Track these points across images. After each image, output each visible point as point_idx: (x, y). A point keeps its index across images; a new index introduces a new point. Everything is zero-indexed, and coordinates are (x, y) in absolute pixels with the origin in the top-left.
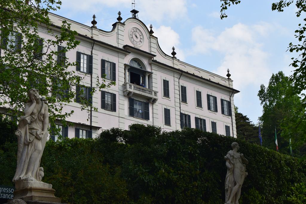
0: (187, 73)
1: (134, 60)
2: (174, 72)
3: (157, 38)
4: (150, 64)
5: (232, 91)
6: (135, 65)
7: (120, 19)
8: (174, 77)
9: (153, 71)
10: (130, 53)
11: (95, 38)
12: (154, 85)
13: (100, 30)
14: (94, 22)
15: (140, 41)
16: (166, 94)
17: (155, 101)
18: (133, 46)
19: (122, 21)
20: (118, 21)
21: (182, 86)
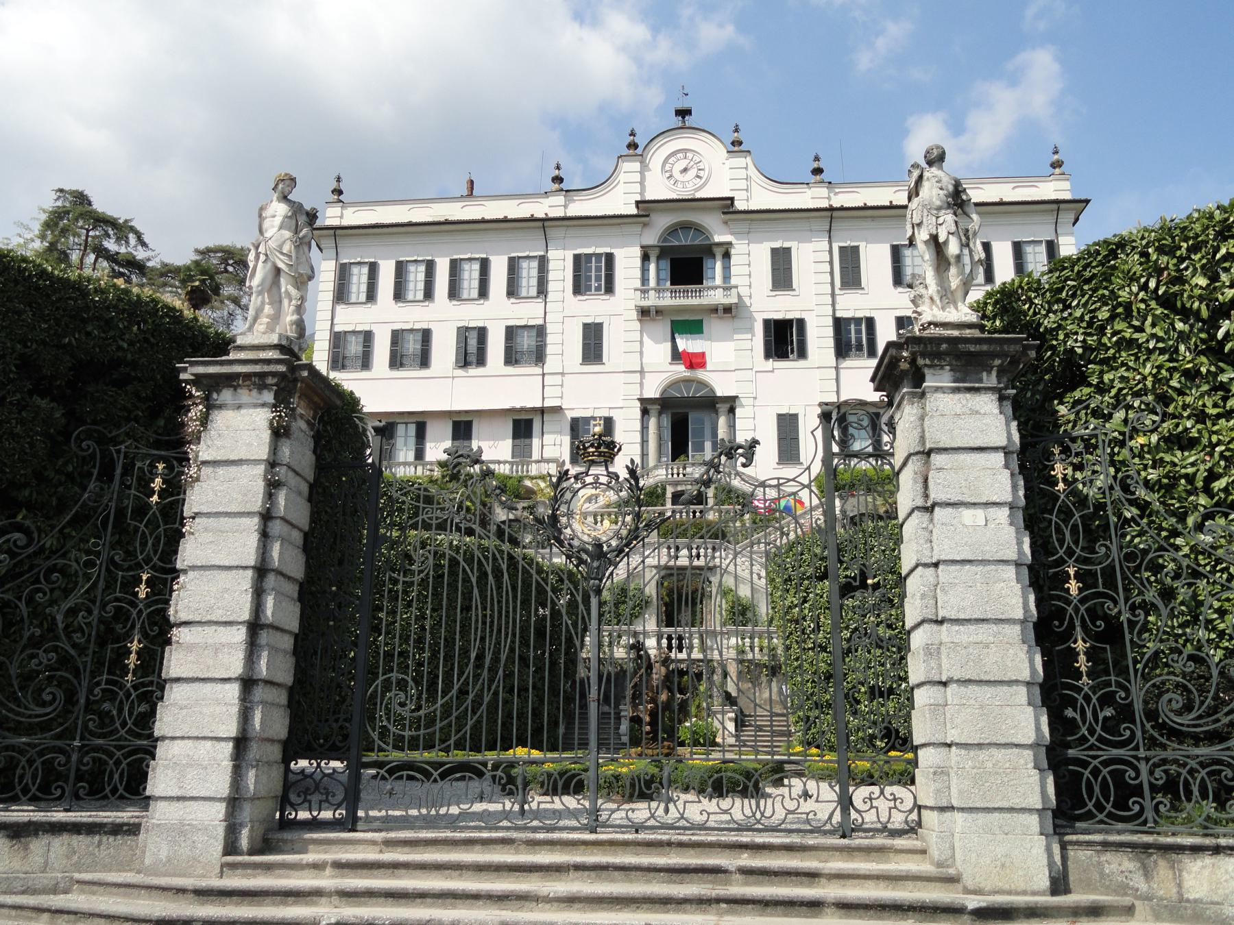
2: (808, 218)
3: (749, 152)
4: (726, 223)
5: (1055, 206)
7: (633, 146)
10: (647, 216)
12: (734, 270)
13: (567, 191)
15: (698, 176)
18: (674, 196)
19: (639, 151)
20: (626, 152)
21: (841, 248)
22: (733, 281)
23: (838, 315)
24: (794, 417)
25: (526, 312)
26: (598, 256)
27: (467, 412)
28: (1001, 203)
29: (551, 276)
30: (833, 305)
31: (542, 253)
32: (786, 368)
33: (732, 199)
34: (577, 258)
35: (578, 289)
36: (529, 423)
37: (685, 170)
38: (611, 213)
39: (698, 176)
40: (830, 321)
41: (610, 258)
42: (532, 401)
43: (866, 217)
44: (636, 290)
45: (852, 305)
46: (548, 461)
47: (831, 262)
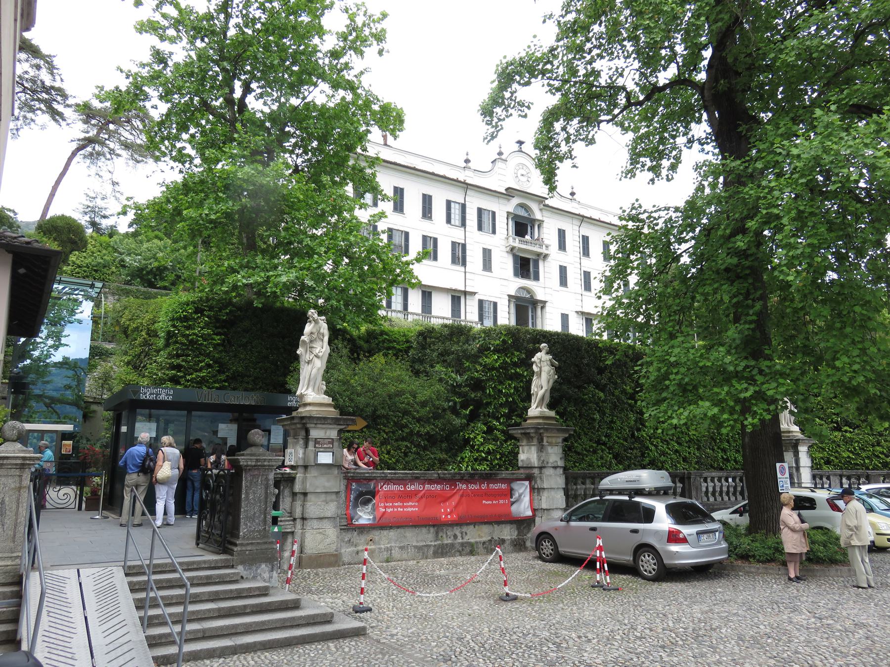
0: (590, 218)
1: (522, 206)
4: (541, 210)
6: (522, 213)
7: (500, 154)
11: (469, 181)
14: (467, 161)
16: (562, 246)
17: (546, 256)
19: (503, 157)
25: (457, 235)
27: (429, 286)
36: (459, 298)
41: (494, 213)
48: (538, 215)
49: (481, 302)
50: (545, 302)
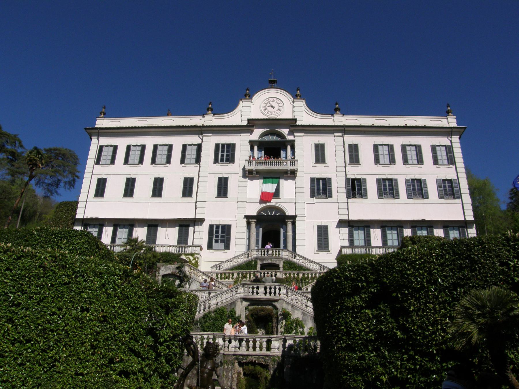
5: (451, 130)
8: (334, 136)
9: (297, 139)
10: (253, 126)
12: (296, 154)
15: (279, 110)
21: (350, 146)
22: (296, 158)
23: (348, 176)
24: (326, 228)
26: (229, 145)
28: (424, 127)
29: (203, 154)
30: (346, 172)
31: (200, 142)
32: (320, 203)
33: (295, 120)
34: (217, 146)
35: (216, 161)
37: (272, 107)
38: (235, 124)
39: (279, 110)
40: (344, 180)
41: (234, 145)
42: (190, 216)
43: (361, 131)
44: (246, 161)
45: (354, 172)
46: (196, 246)
47: (344, 151)
48: (290, 138)
49: (211, 227)
50: (294, 218)
